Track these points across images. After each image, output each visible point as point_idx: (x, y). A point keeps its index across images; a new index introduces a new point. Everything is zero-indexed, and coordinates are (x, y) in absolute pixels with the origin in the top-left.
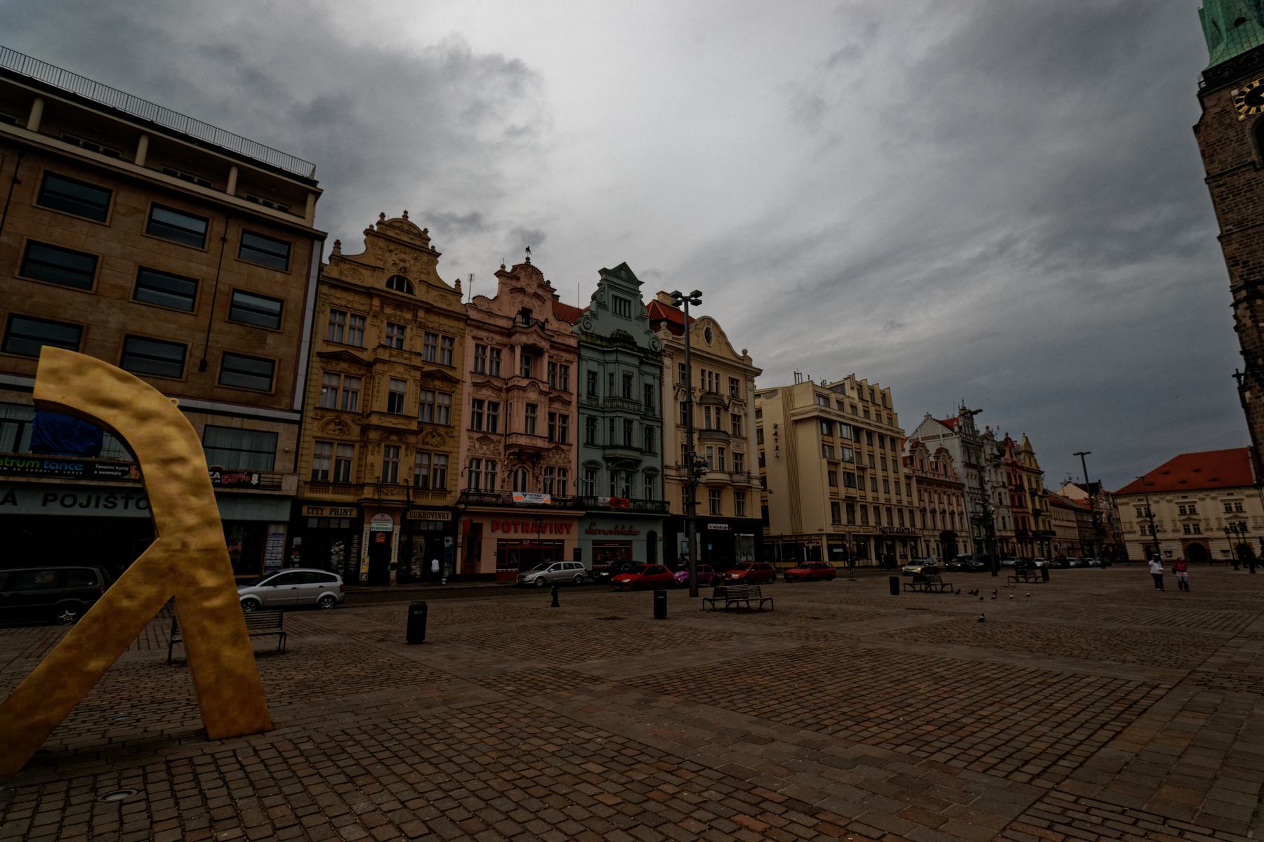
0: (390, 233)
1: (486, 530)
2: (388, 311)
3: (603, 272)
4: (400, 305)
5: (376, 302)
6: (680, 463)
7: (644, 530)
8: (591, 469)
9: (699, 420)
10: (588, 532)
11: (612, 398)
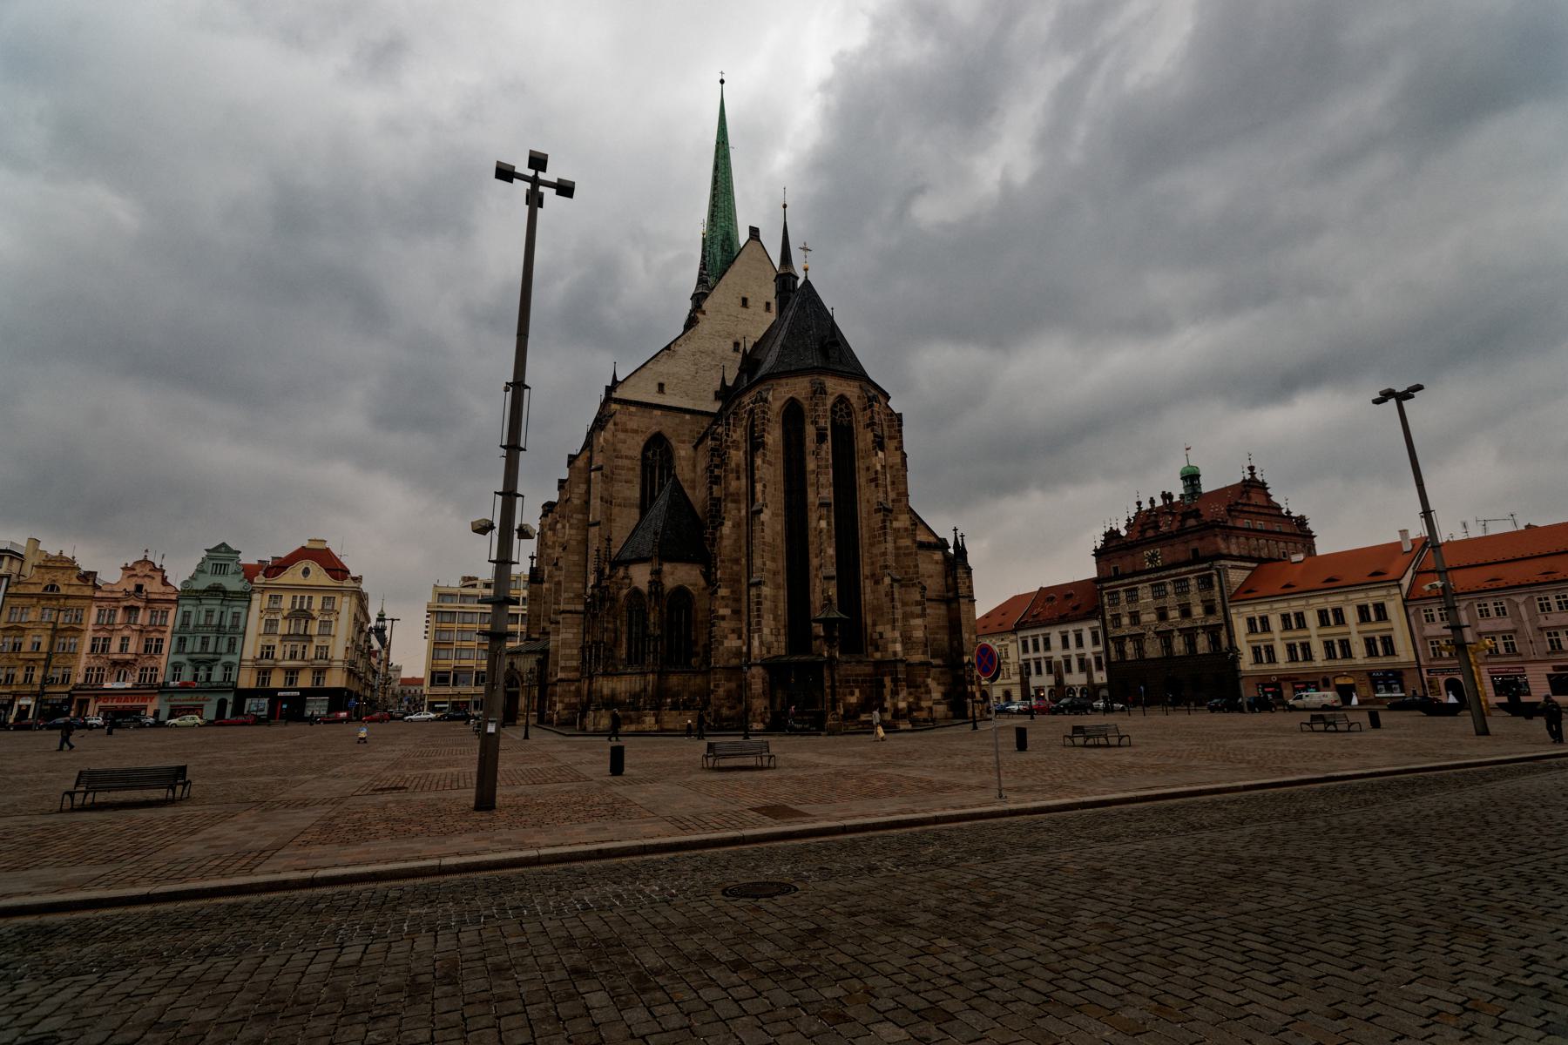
4: (49, 599)
7: (215, 699)
9: (283, 628)
11: (197, 626)
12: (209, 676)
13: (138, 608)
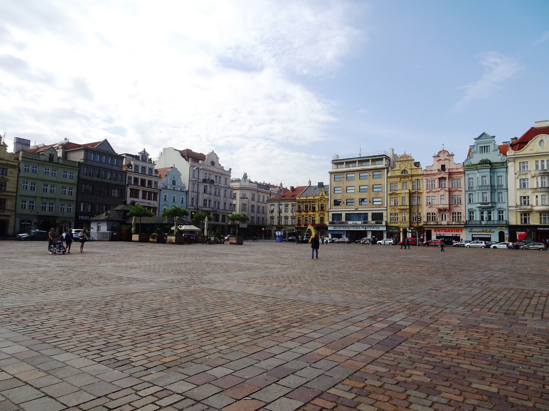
0: (402, 159)
1: (433, 232)
2: (402, 179)
3: (475, 139)
4: (405, 177)
5: (399, 179)
6: (519, 204)
8: (471, 212)
10: (471, 232)
12: (490, 217)
13: (445, 178)
